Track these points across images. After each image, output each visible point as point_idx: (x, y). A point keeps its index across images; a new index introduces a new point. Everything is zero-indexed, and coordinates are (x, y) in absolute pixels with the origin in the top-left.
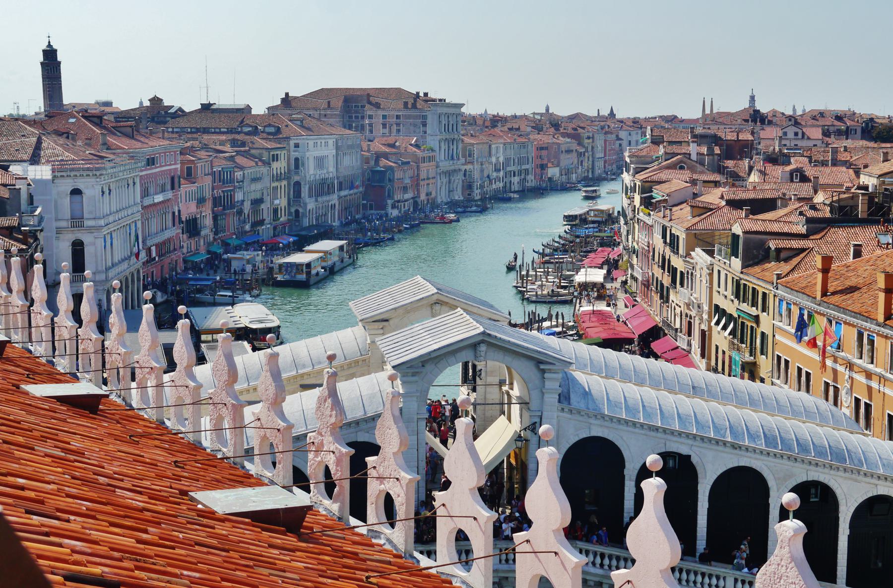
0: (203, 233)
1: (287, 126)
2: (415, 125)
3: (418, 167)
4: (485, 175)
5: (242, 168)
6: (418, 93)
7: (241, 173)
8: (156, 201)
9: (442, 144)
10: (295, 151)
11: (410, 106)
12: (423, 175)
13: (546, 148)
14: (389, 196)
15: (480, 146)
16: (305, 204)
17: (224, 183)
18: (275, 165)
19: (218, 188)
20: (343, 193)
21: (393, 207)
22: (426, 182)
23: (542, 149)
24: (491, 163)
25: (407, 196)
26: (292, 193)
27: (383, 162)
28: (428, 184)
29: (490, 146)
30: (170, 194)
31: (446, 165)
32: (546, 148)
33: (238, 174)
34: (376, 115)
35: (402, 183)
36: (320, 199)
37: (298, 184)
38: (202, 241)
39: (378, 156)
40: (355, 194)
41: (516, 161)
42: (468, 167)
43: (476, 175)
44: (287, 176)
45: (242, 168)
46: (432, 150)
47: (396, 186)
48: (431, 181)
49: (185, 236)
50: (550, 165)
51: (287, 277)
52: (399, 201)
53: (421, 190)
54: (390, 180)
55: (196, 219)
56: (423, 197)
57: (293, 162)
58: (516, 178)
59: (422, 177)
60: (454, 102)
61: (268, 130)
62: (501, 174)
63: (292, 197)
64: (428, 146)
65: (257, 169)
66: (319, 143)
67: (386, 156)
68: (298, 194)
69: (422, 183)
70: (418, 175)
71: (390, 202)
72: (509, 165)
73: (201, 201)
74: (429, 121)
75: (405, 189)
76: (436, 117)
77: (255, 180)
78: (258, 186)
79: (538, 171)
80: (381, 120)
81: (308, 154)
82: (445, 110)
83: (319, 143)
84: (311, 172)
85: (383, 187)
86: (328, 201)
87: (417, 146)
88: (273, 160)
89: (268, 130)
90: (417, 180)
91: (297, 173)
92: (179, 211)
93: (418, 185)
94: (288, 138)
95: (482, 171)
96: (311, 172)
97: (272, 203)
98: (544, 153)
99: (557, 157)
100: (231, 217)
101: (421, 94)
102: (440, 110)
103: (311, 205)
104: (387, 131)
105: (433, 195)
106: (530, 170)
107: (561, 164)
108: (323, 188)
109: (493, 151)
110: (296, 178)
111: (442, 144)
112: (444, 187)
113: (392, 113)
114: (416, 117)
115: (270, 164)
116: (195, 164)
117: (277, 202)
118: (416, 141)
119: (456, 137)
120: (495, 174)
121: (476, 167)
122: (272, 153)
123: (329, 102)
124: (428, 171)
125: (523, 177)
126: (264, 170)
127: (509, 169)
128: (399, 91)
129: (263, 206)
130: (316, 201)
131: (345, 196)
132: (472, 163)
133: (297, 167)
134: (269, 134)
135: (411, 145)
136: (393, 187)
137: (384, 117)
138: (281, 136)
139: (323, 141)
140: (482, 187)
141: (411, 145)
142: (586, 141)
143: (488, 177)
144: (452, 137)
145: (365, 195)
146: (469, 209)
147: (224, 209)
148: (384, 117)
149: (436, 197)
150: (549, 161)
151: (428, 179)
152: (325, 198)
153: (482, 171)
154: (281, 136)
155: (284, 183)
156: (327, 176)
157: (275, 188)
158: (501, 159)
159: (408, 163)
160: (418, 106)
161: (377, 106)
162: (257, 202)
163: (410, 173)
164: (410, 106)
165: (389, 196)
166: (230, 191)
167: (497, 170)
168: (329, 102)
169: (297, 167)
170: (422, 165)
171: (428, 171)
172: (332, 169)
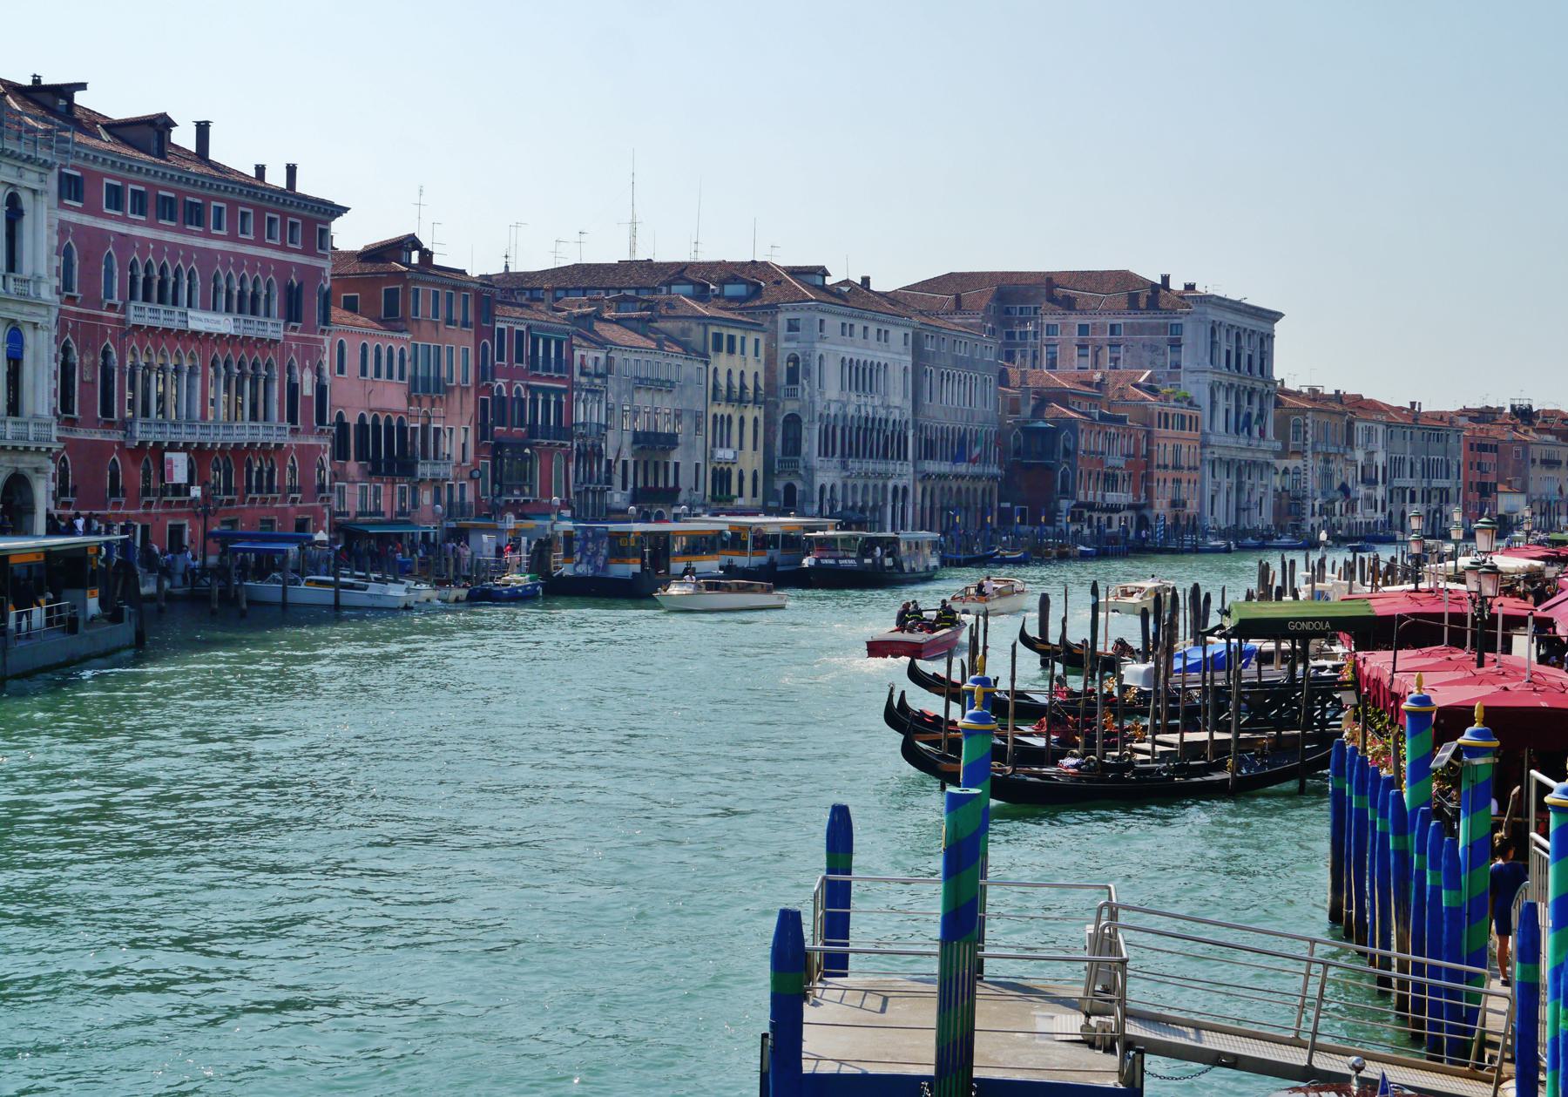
0: (424, 470)
1: (778, 283)
2: (1154, 349)
3: (1149, 433)
4: (1336, 485)
5: (602, 343)
6: (1166, 279)
7: (602, 355)
8: (194, 325)
10: (788, 339)
11: (1143, 303)
12: (1163, 454)
13: (1495, 449)
14: (1064, 490)
15: (1324, 419)
16: (810, 471)
17: (534, 364)
18: (722, 362)
19: (511, 374)
20: (932, 466)
21: (1076, 517)
23: (1483, 448)
24: (1354, 462)
25: (1112, 497)
27: (1056, 409)
28: (1178, 481)
29: (1350, 424)
30: (272, 328)
31: (1225, 443)
32: (1495, 449)
33: (586, 355)
34: (1064, 325)
35: (1101, 463)
36: (853, 464)
37: (793, 421)
38: (426, 497)
39: (1044, 398)
40: (976, 477)
41: (1418, 466)
42: (1292, 463)
43: (1312, 482)
44: (766, 397)
45: (602, 343)
46: (1191, 403)
47: (1083, 467)
48: (1185, 475)
49: (353, 467)
50: (1500, 487)
51: (581, 569)
52: (1091, 507)
53: (1158, 490)
54: (1067, 453)
55: (402, 430)
56: (1161, 507)
57: (782, 367)
58: (1417, 505)
59: (1159, 459)
60: (1254, 300)
61: (730, 290)
62: (1380, 492)
63: (778, 453)
64: (1180, 394)
65: (659, 358)
66: (858, 328)
67: (1062, 397)
68: (793, 445)
69: (1159, 474)
70: (1149, 454)
71: (1065, 504)
72: (1397, 472)
73: (428, 387)
74: (1187, 338)
75: (1110, 481)
76: (1204, 332)
78: (666, 403)
79: (1474, 496)
80: (1076, 337)
81: (820, 348)
82: (1230, 318)
83: (858, 328)
84: (830, 394)
85: (1050, 470)
86: (886, 476)
87: (1152, 390)
88: (718, 349)
89: (730, 290)
90: (1148, 465)
91: (792, 395)
92: (321, 390)
93: (1148, 477)
94: (774, 308)
95: (1327, 476)
96: (830, 394)
97: (709, 456)
98: (1489, 458)
99: (1521, 470)
100: (557, 461)
101: (1176, 285)
102: (1214, 315)
103: (827, 475)
104: (1088, 362)
106: (1453, 492)
107: (1532, 488)
108: (863, 439)
109: (1359, 437)
110: (790, 407)
112: (1222, 498)
113: (1102, 320)
114: (1155, 329)
115: (707, 356)
116: (406, 283)
117: (725, 454)
118: (1150, 379)
119: (1259, 385)
120: (1362, 491)
121: (1310, 463)
122: (713, 329)
123: (958, 299)
124: (1177, 450)
125: (1433, 506)
126: (690, 367)
127: (1397, 482)
128: (1124, 280)
129: (676, 456)
130: (844, 467)
131: (940, 476)
132: (1300, 453)
133: (793, 377)
134: (732, 299)
135: (1137, 386)
136: (1073, 468)
137: (1083, 329)
138: (758, 303)
140: (1326, 511)
141: (1137, 386)
143: (1344, 489)
144: (1248, 383)
145: (1007, 486)
146: (1275, 542)
147: (533, 430)
148: (1083, 329)
149: (1200, 515)
150: (1501, 479)
151: (1177, 467)
152: (870, 465)
153: (1327, 476)
154: (758, 303)
155: (752, 413)
156: (882, 413)
157: (723, 422)
158: (1380, 458)
159: (1122, 420)
160: (1163, 303)
161: (1069, 304)
162: (653, 444)
163: (1124, 444)
164: (1143, 303)
165: (1064, 490)
166: (558, 392)
167: (1370, 482)
168: (958, 299)
169: (793, 377)
170: (1160, 431)
171: (1177, 450)
172: (896, 400)
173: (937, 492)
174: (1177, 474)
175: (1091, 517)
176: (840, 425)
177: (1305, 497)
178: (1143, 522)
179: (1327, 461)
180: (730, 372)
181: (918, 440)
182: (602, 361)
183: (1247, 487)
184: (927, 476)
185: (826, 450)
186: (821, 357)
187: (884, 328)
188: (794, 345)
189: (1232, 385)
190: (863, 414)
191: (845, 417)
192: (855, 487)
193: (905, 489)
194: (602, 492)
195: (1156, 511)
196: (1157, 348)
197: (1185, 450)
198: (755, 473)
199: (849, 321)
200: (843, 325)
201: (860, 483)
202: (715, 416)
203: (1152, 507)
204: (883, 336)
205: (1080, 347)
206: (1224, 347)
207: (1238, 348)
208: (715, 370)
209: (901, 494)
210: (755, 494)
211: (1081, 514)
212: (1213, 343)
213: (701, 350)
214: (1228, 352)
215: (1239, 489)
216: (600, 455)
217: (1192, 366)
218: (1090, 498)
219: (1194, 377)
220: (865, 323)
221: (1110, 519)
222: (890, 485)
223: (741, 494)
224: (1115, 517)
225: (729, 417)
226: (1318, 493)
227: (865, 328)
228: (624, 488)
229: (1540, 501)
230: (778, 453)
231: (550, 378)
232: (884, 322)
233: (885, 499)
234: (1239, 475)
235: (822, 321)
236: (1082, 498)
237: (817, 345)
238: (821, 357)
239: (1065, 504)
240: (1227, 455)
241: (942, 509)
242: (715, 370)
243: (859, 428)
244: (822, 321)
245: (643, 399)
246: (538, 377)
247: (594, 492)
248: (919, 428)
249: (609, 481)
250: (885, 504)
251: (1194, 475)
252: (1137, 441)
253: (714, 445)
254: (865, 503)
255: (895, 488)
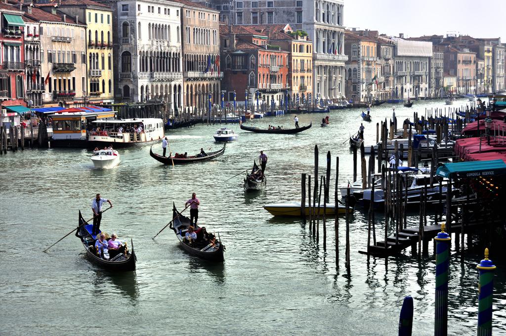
7: (37, 25)
9: (321, 35)
16: (136, 78)
20: (191, 74)
22: (299, 74)
25: (275, 86)
26: (120, 66)
28: (302, 77)
36: (157, 75)
37: (127, 54)
47: (260, 71)
48: (306, 74)
52: (264, 91)
56: (296, 89)
59: (294, 67)
63: (120, 71)
66: (156, 9)
69: (294, 74)
70: (290, 64)
75: (273, 78)
77: (64, 40)
78: (66, 48)
83: (156, 9)
93: (289, 77)
96: (144, 42)
105: (309, 89)
107: (460, 74)
110: (125, 48)
111: (321, 35)
115: (86, 24)
119: (337, 30)
124: (302, 62)
129: (73, 74)
133: (125, 34)
139: (163, 8)
142: (486, 54)
144: (333, 29)
145: (224, 83)
151: (302, 70)
157: (94, 57)
162: (62, 69)
171: (302, 62)
173: (194, 87)
174: (302, 74)
175: (264, 96)
176: (149, 55)
177: (359, 82)
178: (287, 98)
179: (368, 64)
180: (96, 32)
181: (184, 62)
182: (37, 29)
183: (334, 78)
184: (189, 79)
185: (143, 69)
186: (139, 23)
187: (167, 8)
188: (126, 17)
189: (325, 30)
190: (160, 50)
191: (151, 52)
192: (157, 86)
193: (180, 86)
194: (40, 94)
195: (293, 92)
196: (291, 13)
197: (306, 62)
198: (110, 81)
199: (151, 5)
200: (149, 7)
201: (159, 85)
202: (91, 53)
203: (291, 90)
204: (167, 12)
205: (253, 13)
206: (322, 11)
207: (328, 12)
208: (90, 31)
209: (178, 88)
210: (110, 92)
211: (260, 95)
212: (317, 10)
213: (83, 22)
214: (324, 14)
215: (330, 79)
216: (38, 75)
217: (308, 21)
218: (264, 88)
219: (308, 27)
220: (159, 6)
221: (273, 96)
222: (173, 84)
223: (104, 92)
224: (275, 96)
225: (97, 54)
226: (365, 81)
227: (159, 8)
228: (50, 91)
229: (463, 79)
230: (120, 71)
231: (13, 38)
232: (167, 5)
233: (170, 92)
234: (330, 73)
235: (139, 5)
236: (260, 87)
237: (137, 17)
238: (139, 23)
239: (252, 90)
240: (324, 63)
241: (196, 95)
242: (90, 31)
243: (158, 57)
244: (139, 5)
245: (57, 48)
246: (8, 38)
247: (36, 94)
248: (184, 56)
249: (43, 88)
250: (171, 94)
251: (310, 74)
252: (284, 58)
253: (90, 68)
254: (162, 93)
255: (175, 85)
